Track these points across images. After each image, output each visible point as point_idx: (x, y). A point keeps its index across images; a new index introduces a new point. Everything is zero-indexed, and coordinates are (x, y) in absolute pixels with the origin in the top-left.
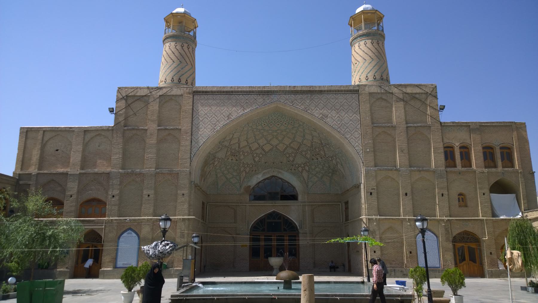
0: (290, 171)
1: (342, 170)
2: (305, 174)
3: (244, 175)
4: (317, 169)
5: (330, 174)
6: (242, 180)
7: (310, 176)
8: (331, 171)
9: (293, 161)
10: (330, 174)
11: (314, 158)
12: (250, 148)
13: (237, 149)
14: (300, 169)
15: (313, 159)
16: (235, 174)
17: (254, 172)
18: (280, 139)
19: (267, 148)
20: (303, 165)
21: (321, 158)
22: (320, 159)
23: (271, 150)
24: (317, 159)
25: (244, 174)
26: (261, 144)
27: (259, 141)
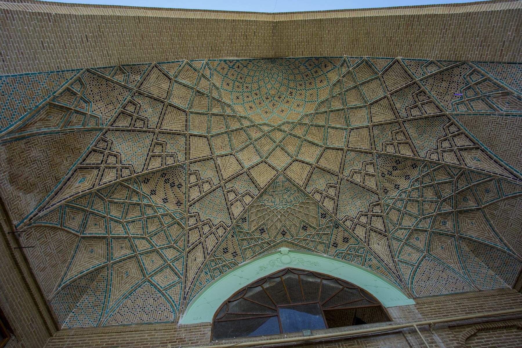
0: (333, 250)
1: (488, 166)
2: (379, 246)
3: (200, 259)
4: (408, 222)
5: (449, 225)
6: (191, 275)
7: (396, 245)
8: (447, 208)
9: (336, 208)
10: (449, 225)
11: (387, 185)
12: (217, 169)
13: (181, 157)
14: (360, 232)
15: (386, 191)
16: (170, 254)
17: (229, 256)
18: (291, 149)
19: (263, 178)
20: (364, 220)
21: (407, 177)
22: (404, 184)
23: (273, 183)
24: (397, 187)
25: (199, 254)
26: (247, 165)
27: (240, 156)
